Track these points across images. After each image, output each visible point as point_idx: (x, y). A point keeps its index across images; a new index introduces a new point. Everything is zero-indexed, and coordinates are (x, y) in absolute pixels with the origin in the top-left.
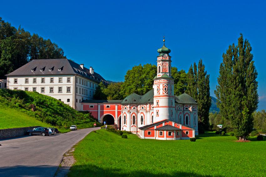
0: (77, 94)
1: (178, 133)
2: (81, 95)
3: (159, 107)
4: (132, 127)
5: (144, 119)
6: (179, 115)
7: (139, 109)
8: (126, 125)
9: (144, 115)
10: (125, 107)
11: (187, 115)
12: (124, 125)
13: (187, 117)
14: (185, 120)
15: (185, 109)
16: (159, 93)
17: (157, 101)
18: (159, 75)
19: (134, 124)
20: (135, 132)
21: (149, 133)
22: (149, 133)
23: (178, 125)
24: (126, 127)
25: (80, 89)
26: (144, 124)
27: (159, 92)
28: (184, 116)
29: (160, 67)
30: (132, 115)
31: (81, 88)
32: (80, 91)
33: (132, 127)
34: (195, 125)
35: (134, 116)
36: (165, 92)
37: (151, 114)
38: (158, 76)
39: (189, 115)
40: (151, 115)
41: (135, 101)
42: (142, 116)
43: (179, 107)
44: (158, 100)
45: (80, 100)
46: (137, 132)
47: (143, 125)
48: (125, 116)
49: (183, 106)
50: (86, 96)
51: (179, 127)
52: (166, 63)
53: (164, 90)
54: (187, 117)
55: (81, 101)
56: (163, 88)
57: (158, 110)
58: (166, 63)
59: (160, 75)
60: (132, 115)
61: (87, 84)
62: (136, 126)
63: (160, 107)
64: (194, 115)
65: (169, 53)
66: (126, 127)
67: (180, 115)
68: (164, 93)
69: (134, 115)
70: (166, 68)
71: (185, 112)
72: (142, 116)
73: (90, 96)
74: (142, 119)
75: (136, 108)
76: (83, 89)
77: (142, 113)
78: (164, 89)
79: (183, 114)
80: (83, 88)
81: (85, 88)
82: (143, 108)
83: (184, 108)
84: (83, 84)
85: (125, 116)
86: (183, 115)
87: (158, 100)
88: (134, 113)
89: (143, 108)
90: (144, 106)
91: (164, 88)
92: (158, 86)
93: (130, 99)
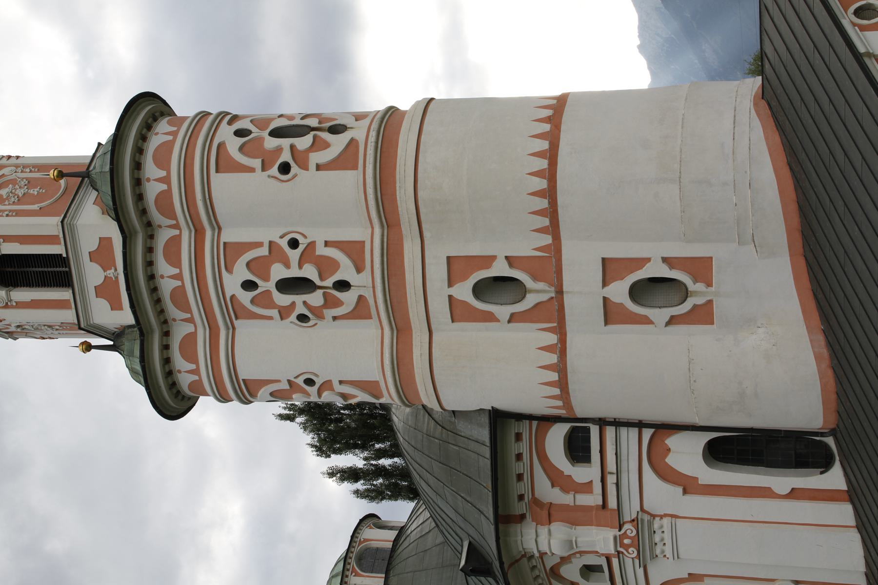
3: (556, 248)
17: (464, 292)
27: (326, 266)
36: (336, 130)
40: (689, 486)
44: (456, 268)
53: (303, 143)
57: (610, 269)
63: (554, 229)
68: (338, 143)
70: (30, 183)
78: (285, 142)
87: (456, 268)
91: (271, 143)
92: (241, 273)
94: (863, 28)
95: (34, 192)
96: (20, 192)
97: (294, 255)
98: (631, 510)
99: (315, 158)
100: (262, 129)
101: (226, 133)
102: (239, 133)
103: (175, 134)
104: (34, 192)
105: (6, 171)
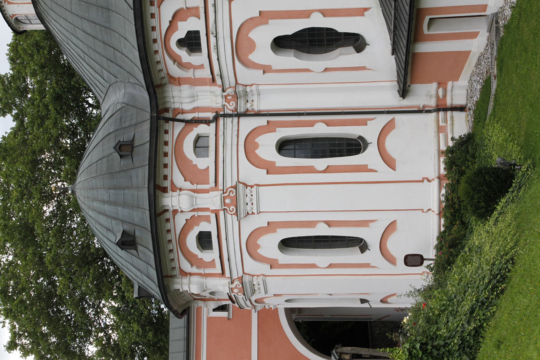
4: (390, 162)
5: (306, 14)
7: (210, 98)
10: (191, 242)
12: (373, 255)
19: (354, 146)
20: (440, 129)
24: (391, 227)
26: (361, 12)
30: (270, 168)
33: (390, 162)
35: (284, 146)
42: (280, 43)
46: (441, 108)
47: (375, 29)
48: (287, 244)
62: (383, 120)
66: (391, 227)
72: (280, 43)
74: (314, 41)
75: (202, 129)
77: (241, 48)
82: (191, 42)
85: (287, 244)
89: (191, 42)
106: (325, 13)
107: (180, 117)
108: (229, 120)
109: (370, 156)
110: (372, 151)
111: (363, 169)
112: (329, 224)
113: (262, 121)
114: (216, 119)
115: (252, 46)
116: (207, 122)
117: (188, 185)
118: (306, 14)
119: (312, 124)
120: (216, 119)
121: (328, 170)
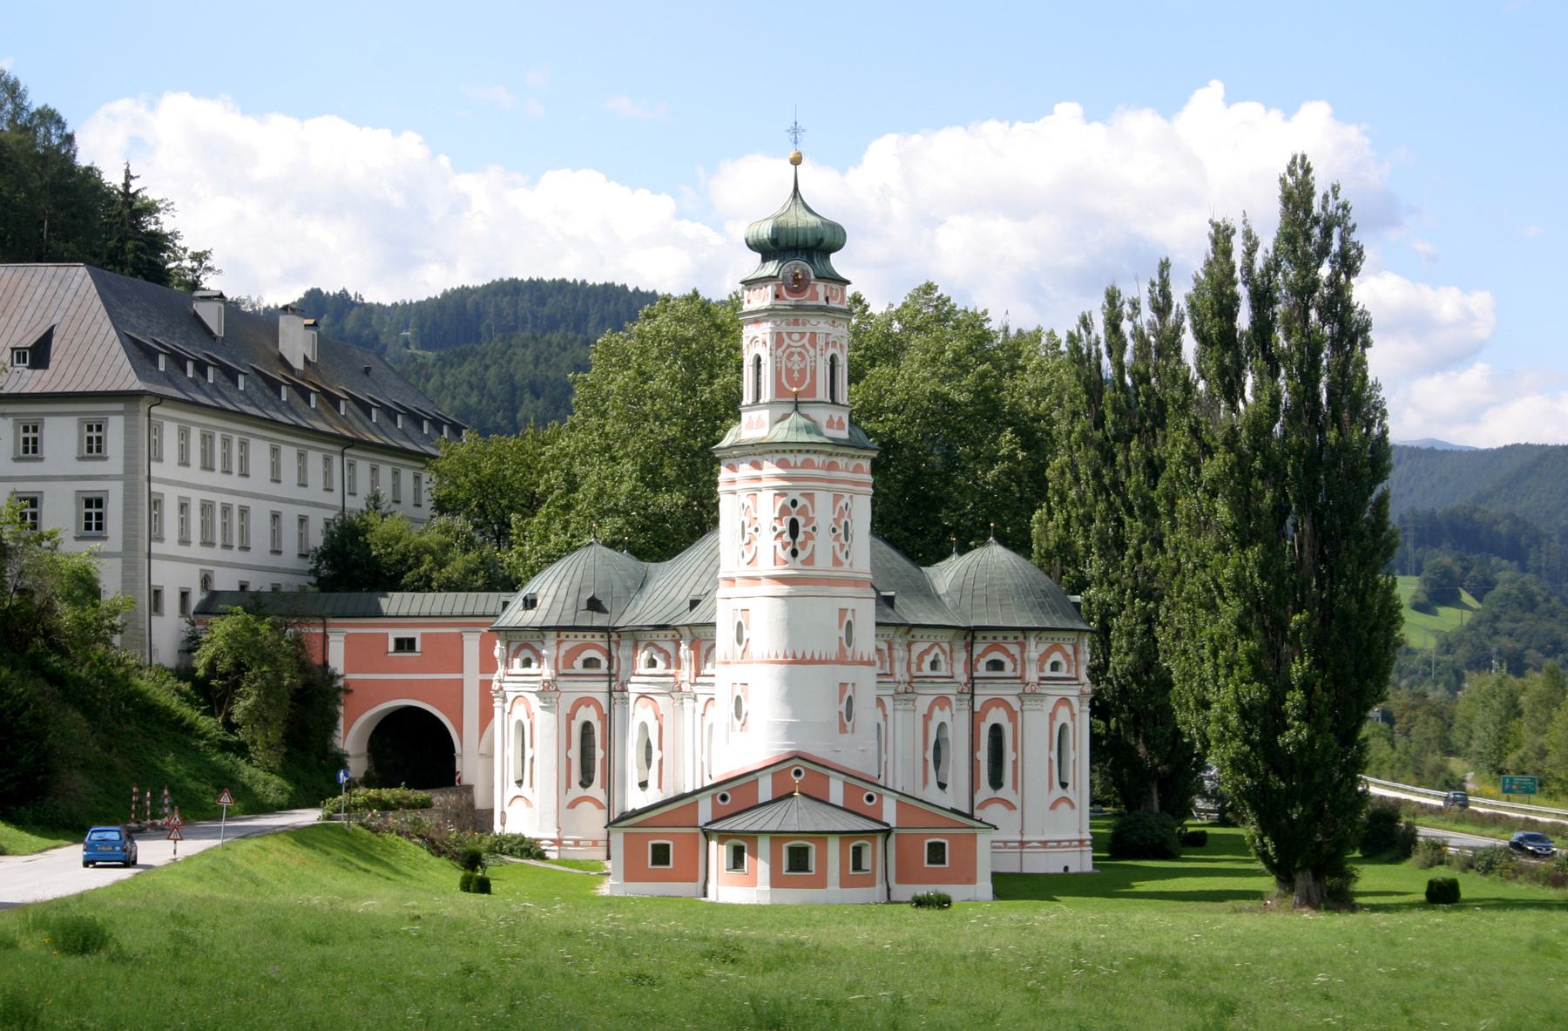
0: (156, 548)
1: (858, 852)
2: (195, 550)
4: (573, 805)
6: (927, 718)
8: (525, 790)
9: (658, 717)
11: (997, 716)
12: (513, 790)
13: (996, 730)
14: (983, 755)
15: (981, 670)
16: (748, 557)
18: (754, 425)
19: (586, 781)
20: (595, 843)
21: (661, 855)
22: (661, 855)
23: (870, 798)
25: (184, 507)
28: (975, 719)
29: (758, 359)
30: (571, 717)
31: (196, 498)
32: (184, 522)
34: (1058, 792)
35: (587, 728)
37: (700, 709)
38: (750, 426)
39: (1012, 715)
41: (594, 605)
43: (929, 659)
45: (184, 595)
48: (520, 725)
49: (970, 647)
50: (235, 555)
51: (880, 806)
52: (802, 335)
54: (996, 730)
55: (196, 598)
56: (779, 519)
58: (802, 335)
59: (760, 424)
60: (571, 717)
61: (244, 460)
64: (1053, 716)
65: (832, 256)
67: (939, 716)
69: (588, 714)
70: (802, 372)
71: (983, 694)
73: (276, 552)
75: (604, 663)
76: (206, 507)
79: (966, 706)
80: (209, 496)
81: (227, 499)
83: (971, 664)
84: (207, 466)
86: (964, 719)
88: (587, 701)
90: (661, 650)
91: (787, 519)
93: (563, 592)
94: (714, 796)
95: (796, 375)
96: (796, 367)
97: (752, 530)
98: (696, 689)
99: (778, 543)
100: (799, 513)
101: (795, 495)
102: (794, 503)
103: (795, 466)
104: (796, 375)
105: (812, 352)
106: (661, 762)
107: (613, 646)
108: (606, 685)
109: (577, 792)
110: (581, 792)
111: (569, 785)
112: (532, 760)
113: (605, 711)
114: (610, 675)
115: (645, 707)
116: (610, 668)
117: (562, 653)
118: (660, 748)
119: (603, 747)
120: (610, 675)
121: (569, 760)
